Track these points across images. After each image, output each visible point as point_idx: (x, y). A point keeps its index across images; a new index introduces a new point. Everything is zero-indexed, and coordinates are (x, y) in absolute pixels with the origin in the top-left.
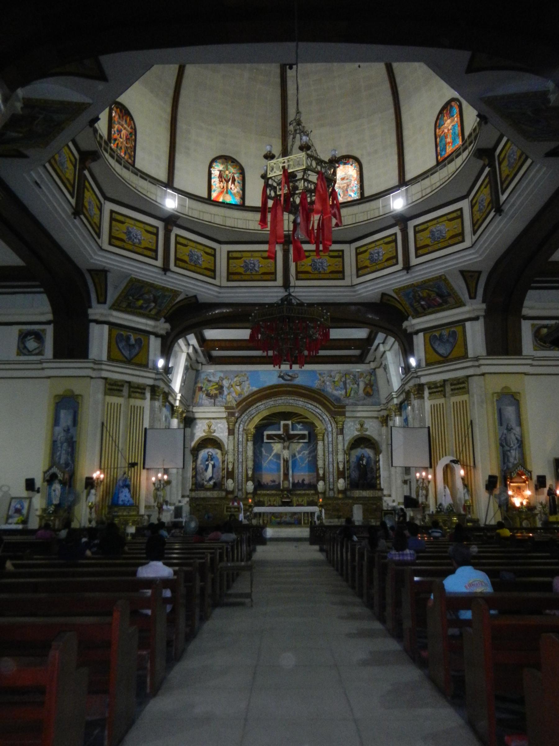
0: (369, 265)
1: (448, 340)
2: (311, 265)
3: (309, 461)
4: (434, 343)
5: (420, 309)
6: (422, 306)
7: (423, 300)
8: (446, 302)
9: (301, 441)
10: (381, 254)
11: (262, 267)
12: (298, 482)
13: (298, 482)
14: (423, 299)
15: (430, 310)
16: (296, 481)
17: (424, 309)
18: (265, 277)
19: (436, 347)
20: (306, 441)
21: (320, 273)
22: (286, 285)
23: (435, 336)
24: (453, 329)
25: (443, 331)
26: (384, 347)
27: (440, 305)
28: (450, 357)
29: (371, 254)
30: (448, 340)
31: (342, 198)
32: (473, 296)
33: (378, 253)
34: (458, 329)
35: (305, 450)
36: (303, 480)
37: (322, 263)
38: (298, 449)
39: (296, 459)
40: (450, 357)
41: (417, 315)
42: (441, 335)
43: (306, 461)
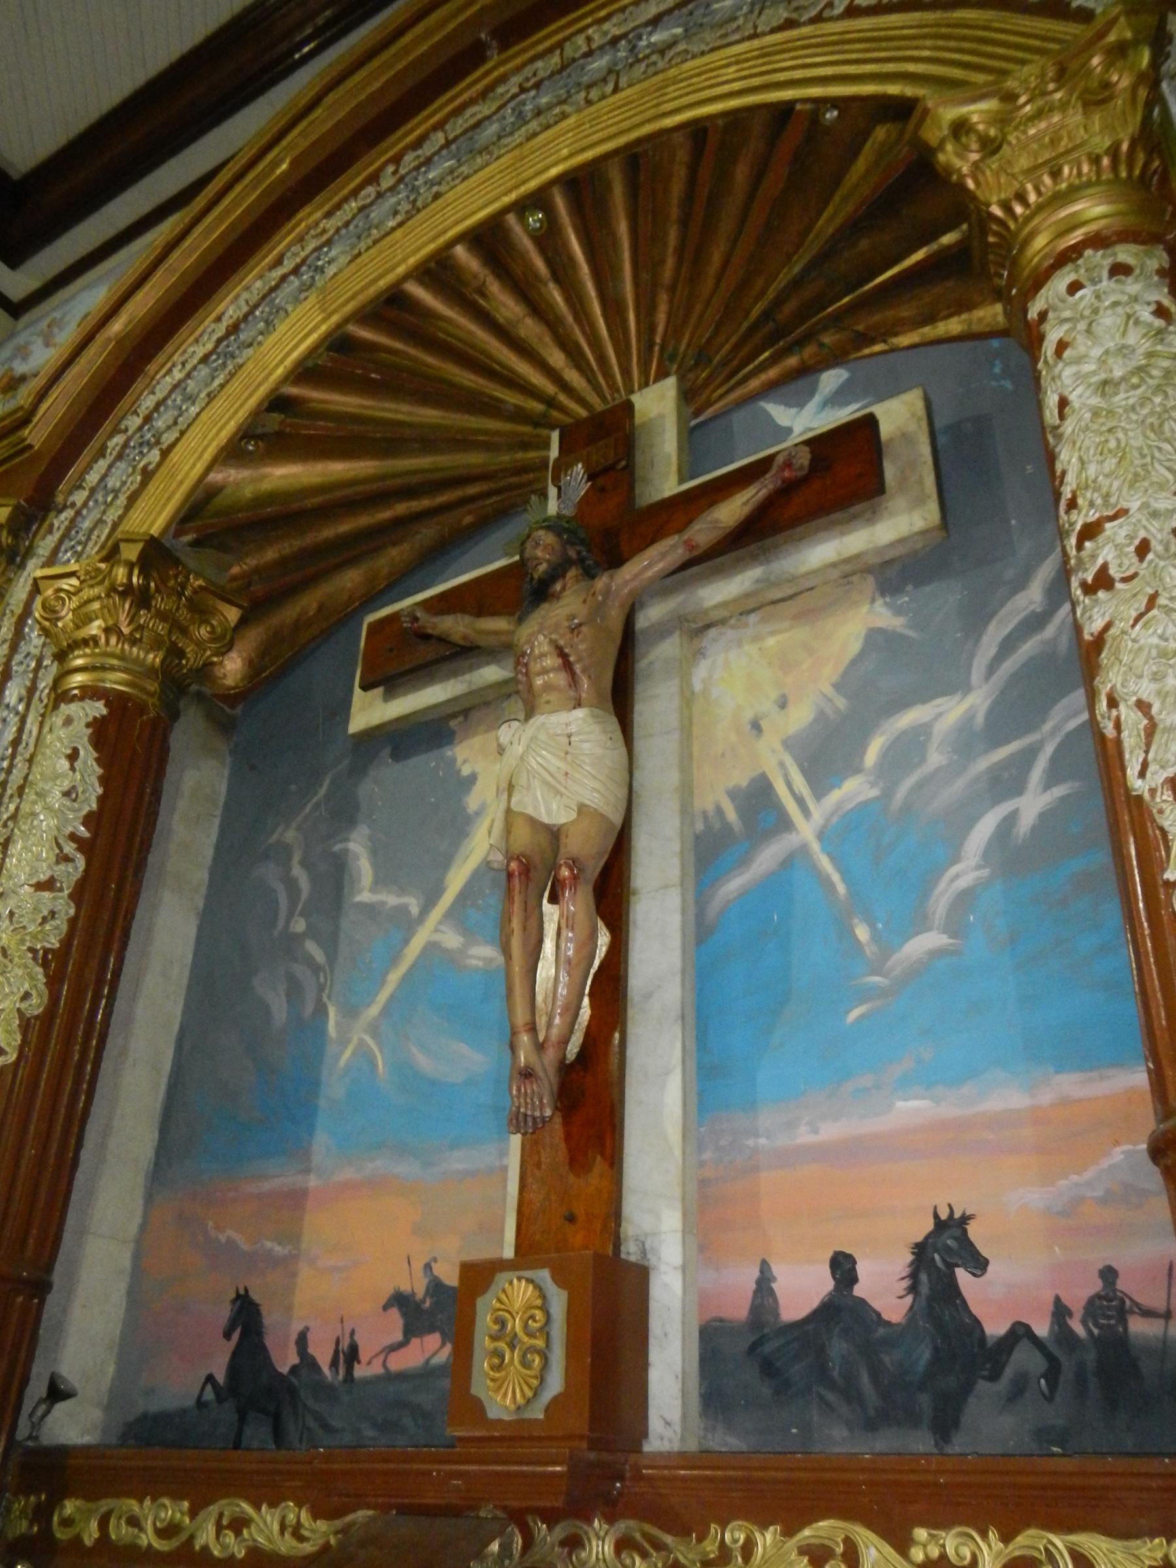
3: (1007, 853)
9: (822, 552)
12: (842, 1309)
13: (842, 1309)
16: (802, 1289)
20: (901, 520)
35: (922, 695)
36: (946, 1249)
38: (800, 717)
39: (798, 857)
43: (966, 872)
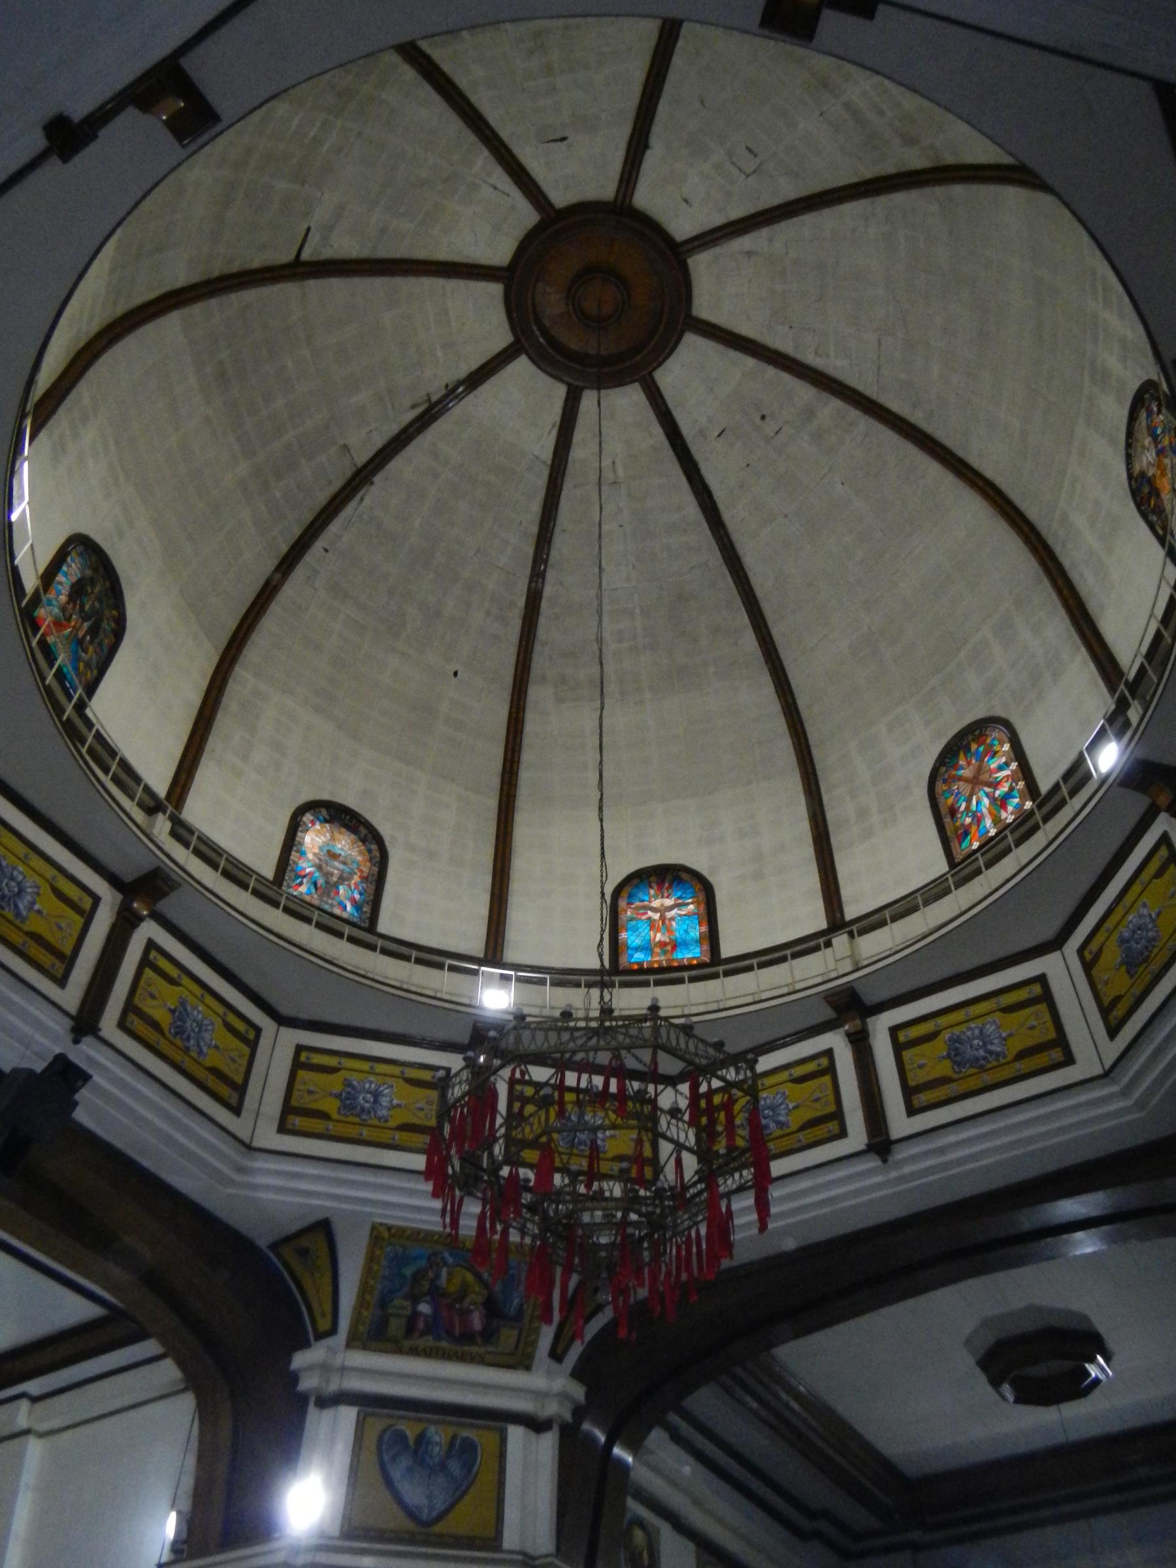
0: (335, 1116)
1: (443, 1466)
2: (173, 1012)
4: (394, 1458)
5: (396, 1326)
6: (415, 1316)
7: (435, 1304)
8: (488, 1335)
10: (384, 1101)
11: (39, 912)
14: (435, 1294)
15: (429, 1341)
17: (410, 1328)
18: (34, 950)
19: (396, 1474)
21: (187, 1050)
22: (85, 1024)
23: (401, 1437)
24: (465, 1433)
25: (432, 1429)
26: (30, 1413)
27: (468, 1337)
28: (438, 1528)
29: (347, 1083)
30: (443, 1466)
31: (321, 896)
32: (557, 1355)
33: (376, 1095)
34: (483, 1438)
37: (200, 1025)
40: (438, 1528)
41: (374, 1334)
42: (421, 1438)
